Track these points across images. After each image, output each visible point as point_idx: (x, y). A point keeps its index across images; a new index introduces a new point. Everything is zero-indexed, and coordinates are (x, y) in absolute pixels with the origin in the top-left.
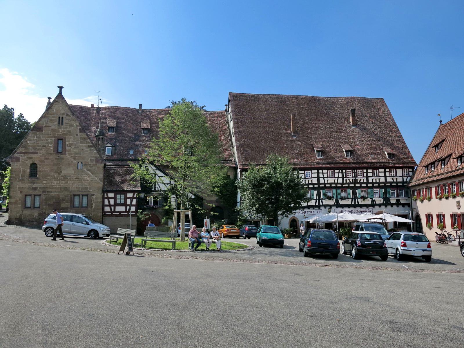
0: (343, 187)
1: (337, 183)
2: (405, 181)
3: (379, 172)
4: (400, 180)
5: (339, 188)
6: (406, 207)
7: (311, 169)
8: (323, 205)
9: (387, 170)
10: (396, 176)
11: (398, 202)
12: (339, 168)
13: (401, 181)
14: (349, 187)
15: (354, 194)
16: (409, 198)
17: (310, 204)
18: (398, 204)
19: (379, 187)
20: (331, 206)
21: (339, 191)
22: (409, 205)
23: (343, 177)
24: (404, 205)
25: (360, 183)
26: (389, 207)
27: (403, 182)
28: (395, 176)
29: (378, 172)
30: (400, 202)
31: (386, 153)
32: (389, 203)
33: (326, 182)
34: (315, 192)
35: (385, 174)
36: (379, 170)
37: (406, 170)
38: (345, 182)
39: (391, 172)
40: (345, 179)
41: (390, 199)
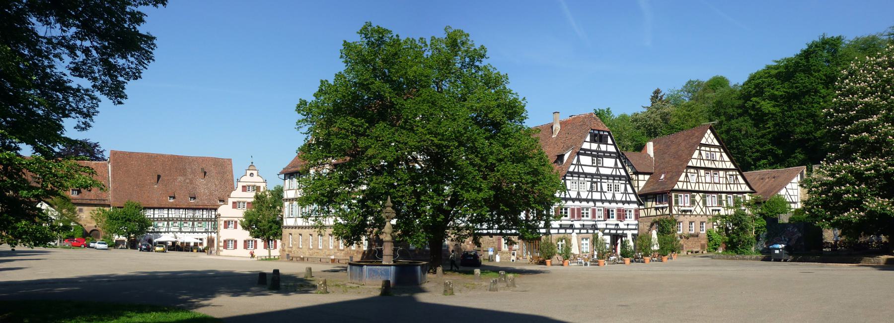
0: (186, 220)
1: (181, 218)
5: (183, 221)
7: (163, 208)
8: (171, 232)
12: (183, 208)
14: (190, 220)
15: (193, 224)
17: (161, 230)
20: (177, 232)
21: (182, 223)
23: (185, 214)
25: (197, 218)
33: (174, 217)
34: (166, 223)
38: (187, 217)
40: (187, 215)
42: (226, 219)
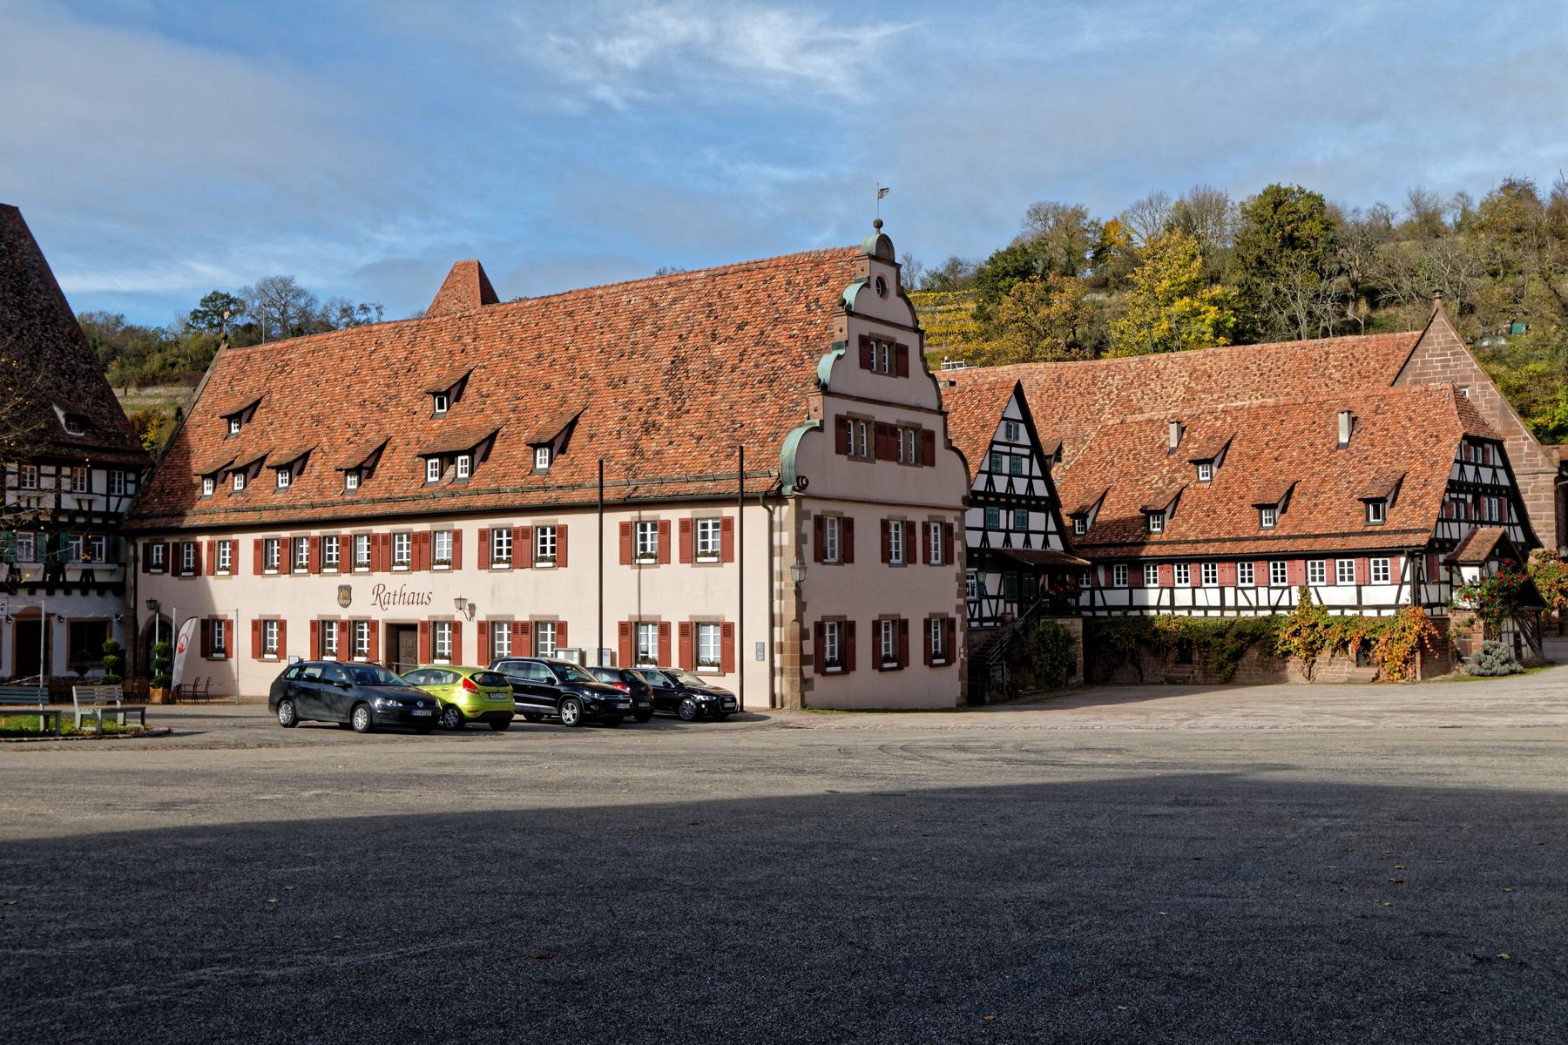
2: (112, 509)
3: (40, 475)
4: (99, 506)
6: (109, 594)
9: (66, 471)
10: (90, 491)
11: (87, 579)
13: (103, 509)
16: (120, 565)
18: (87, 585)
19: (33, 526)
22: (119, 589)
24: (102, 589)
26: (60, 594)
27: (104, 515)
28: (85, 491)
29: (35, 474)
30: (93, 578)
31: (60, 414)
32: (61, 579)
35: (58, 484)
36: (39, 469)
37: (120, 476)
39: (76, 480)
41: (67, 566)
42: (816, 508)
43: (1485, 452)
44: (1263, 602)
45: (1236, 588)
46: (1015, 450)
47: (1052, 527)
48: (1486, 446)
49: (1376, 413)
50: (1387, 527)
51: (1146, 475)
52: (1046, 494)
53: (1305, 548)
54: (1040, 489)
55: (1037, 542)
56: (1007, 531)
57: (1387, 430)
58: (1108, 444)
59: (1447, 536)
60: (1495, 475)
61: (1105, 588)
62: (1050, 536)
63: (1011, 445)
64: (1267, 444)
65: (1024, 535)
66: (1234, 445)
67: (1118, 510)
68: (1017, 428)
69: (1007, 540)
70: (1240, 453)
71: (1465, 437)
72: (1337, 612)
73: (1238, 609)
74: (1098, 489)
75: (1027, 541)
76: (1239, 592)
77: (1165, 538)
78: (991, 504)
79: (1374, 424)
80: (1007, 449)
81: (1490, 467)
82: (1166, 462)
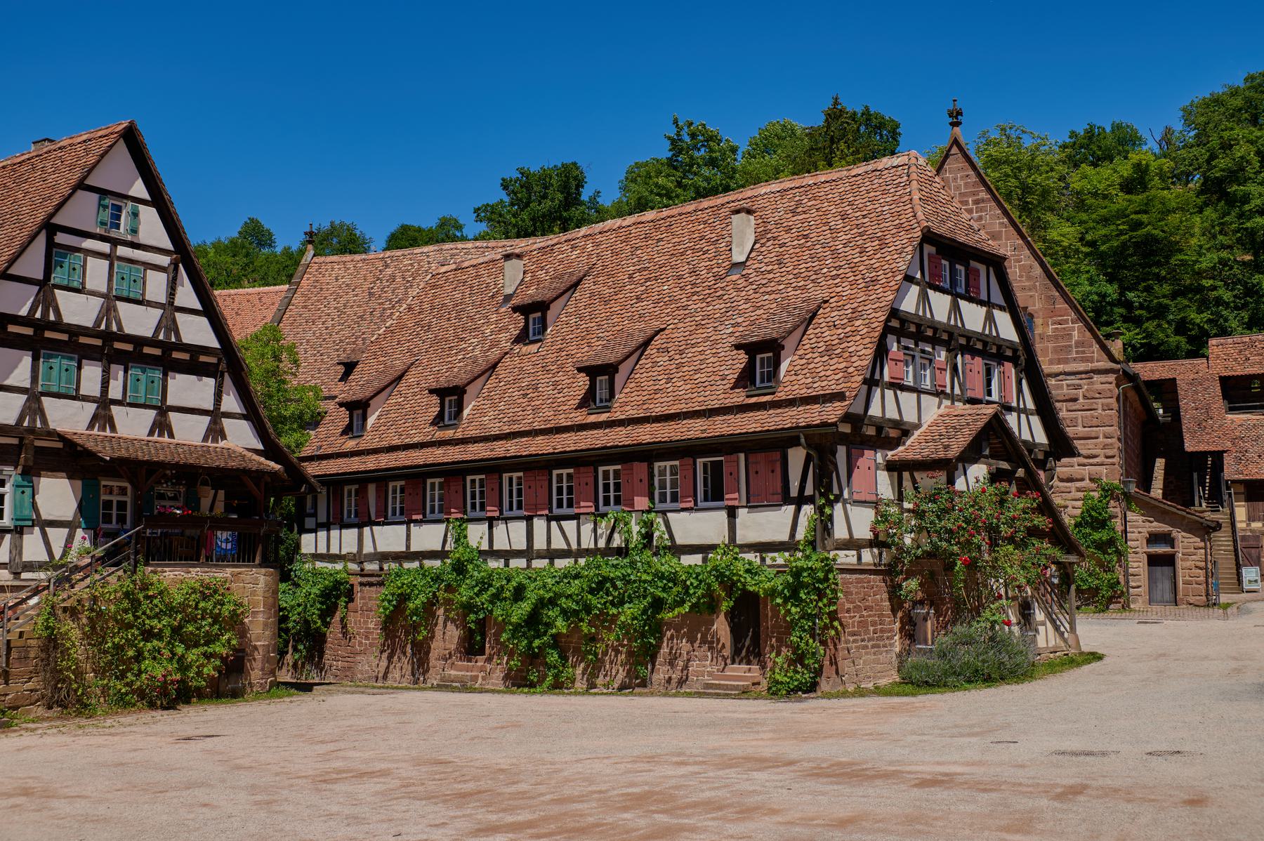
43: (971, 275)
44: (587, 543)
45: (549, 519)
46: (122, 251)
47: (231, 402)
48: (973, 264)
49: (794, 213)
50: (781, 395)
51: (462, 339)
52: (215, 344)
53: (647, 438)
54: (196, 331)
55: (189, 431)
56: (104, 402)
57: (806, 237)
58: (434, 296)
59: (892, 413)
60: (990, 318)
61: (378, 524)
62: (225, 422)
63: (115, 242)
64: (631, 277)
65: (152, 414)
66: (587, 284)
67: (414, 394)
68: (135, 215)
69: (103, 418)
70: (592, 294)
71: (928, 237)
72: (696, 559)
73: (552, 555)
74: (399, 365)
75: (162, 426)
76: (554, 524)
77: (459, 435)
78: (56, 346)
79: (789, 230)
80: (105, 247)
81: (981, 303)
82: (494, 317)
